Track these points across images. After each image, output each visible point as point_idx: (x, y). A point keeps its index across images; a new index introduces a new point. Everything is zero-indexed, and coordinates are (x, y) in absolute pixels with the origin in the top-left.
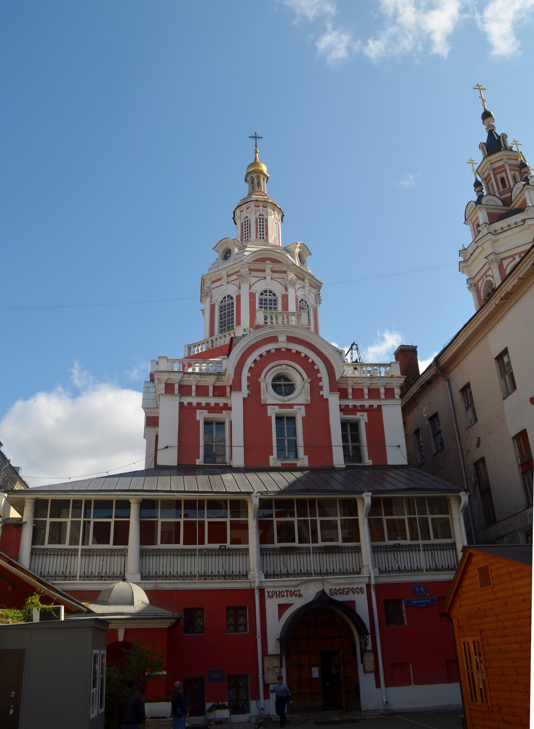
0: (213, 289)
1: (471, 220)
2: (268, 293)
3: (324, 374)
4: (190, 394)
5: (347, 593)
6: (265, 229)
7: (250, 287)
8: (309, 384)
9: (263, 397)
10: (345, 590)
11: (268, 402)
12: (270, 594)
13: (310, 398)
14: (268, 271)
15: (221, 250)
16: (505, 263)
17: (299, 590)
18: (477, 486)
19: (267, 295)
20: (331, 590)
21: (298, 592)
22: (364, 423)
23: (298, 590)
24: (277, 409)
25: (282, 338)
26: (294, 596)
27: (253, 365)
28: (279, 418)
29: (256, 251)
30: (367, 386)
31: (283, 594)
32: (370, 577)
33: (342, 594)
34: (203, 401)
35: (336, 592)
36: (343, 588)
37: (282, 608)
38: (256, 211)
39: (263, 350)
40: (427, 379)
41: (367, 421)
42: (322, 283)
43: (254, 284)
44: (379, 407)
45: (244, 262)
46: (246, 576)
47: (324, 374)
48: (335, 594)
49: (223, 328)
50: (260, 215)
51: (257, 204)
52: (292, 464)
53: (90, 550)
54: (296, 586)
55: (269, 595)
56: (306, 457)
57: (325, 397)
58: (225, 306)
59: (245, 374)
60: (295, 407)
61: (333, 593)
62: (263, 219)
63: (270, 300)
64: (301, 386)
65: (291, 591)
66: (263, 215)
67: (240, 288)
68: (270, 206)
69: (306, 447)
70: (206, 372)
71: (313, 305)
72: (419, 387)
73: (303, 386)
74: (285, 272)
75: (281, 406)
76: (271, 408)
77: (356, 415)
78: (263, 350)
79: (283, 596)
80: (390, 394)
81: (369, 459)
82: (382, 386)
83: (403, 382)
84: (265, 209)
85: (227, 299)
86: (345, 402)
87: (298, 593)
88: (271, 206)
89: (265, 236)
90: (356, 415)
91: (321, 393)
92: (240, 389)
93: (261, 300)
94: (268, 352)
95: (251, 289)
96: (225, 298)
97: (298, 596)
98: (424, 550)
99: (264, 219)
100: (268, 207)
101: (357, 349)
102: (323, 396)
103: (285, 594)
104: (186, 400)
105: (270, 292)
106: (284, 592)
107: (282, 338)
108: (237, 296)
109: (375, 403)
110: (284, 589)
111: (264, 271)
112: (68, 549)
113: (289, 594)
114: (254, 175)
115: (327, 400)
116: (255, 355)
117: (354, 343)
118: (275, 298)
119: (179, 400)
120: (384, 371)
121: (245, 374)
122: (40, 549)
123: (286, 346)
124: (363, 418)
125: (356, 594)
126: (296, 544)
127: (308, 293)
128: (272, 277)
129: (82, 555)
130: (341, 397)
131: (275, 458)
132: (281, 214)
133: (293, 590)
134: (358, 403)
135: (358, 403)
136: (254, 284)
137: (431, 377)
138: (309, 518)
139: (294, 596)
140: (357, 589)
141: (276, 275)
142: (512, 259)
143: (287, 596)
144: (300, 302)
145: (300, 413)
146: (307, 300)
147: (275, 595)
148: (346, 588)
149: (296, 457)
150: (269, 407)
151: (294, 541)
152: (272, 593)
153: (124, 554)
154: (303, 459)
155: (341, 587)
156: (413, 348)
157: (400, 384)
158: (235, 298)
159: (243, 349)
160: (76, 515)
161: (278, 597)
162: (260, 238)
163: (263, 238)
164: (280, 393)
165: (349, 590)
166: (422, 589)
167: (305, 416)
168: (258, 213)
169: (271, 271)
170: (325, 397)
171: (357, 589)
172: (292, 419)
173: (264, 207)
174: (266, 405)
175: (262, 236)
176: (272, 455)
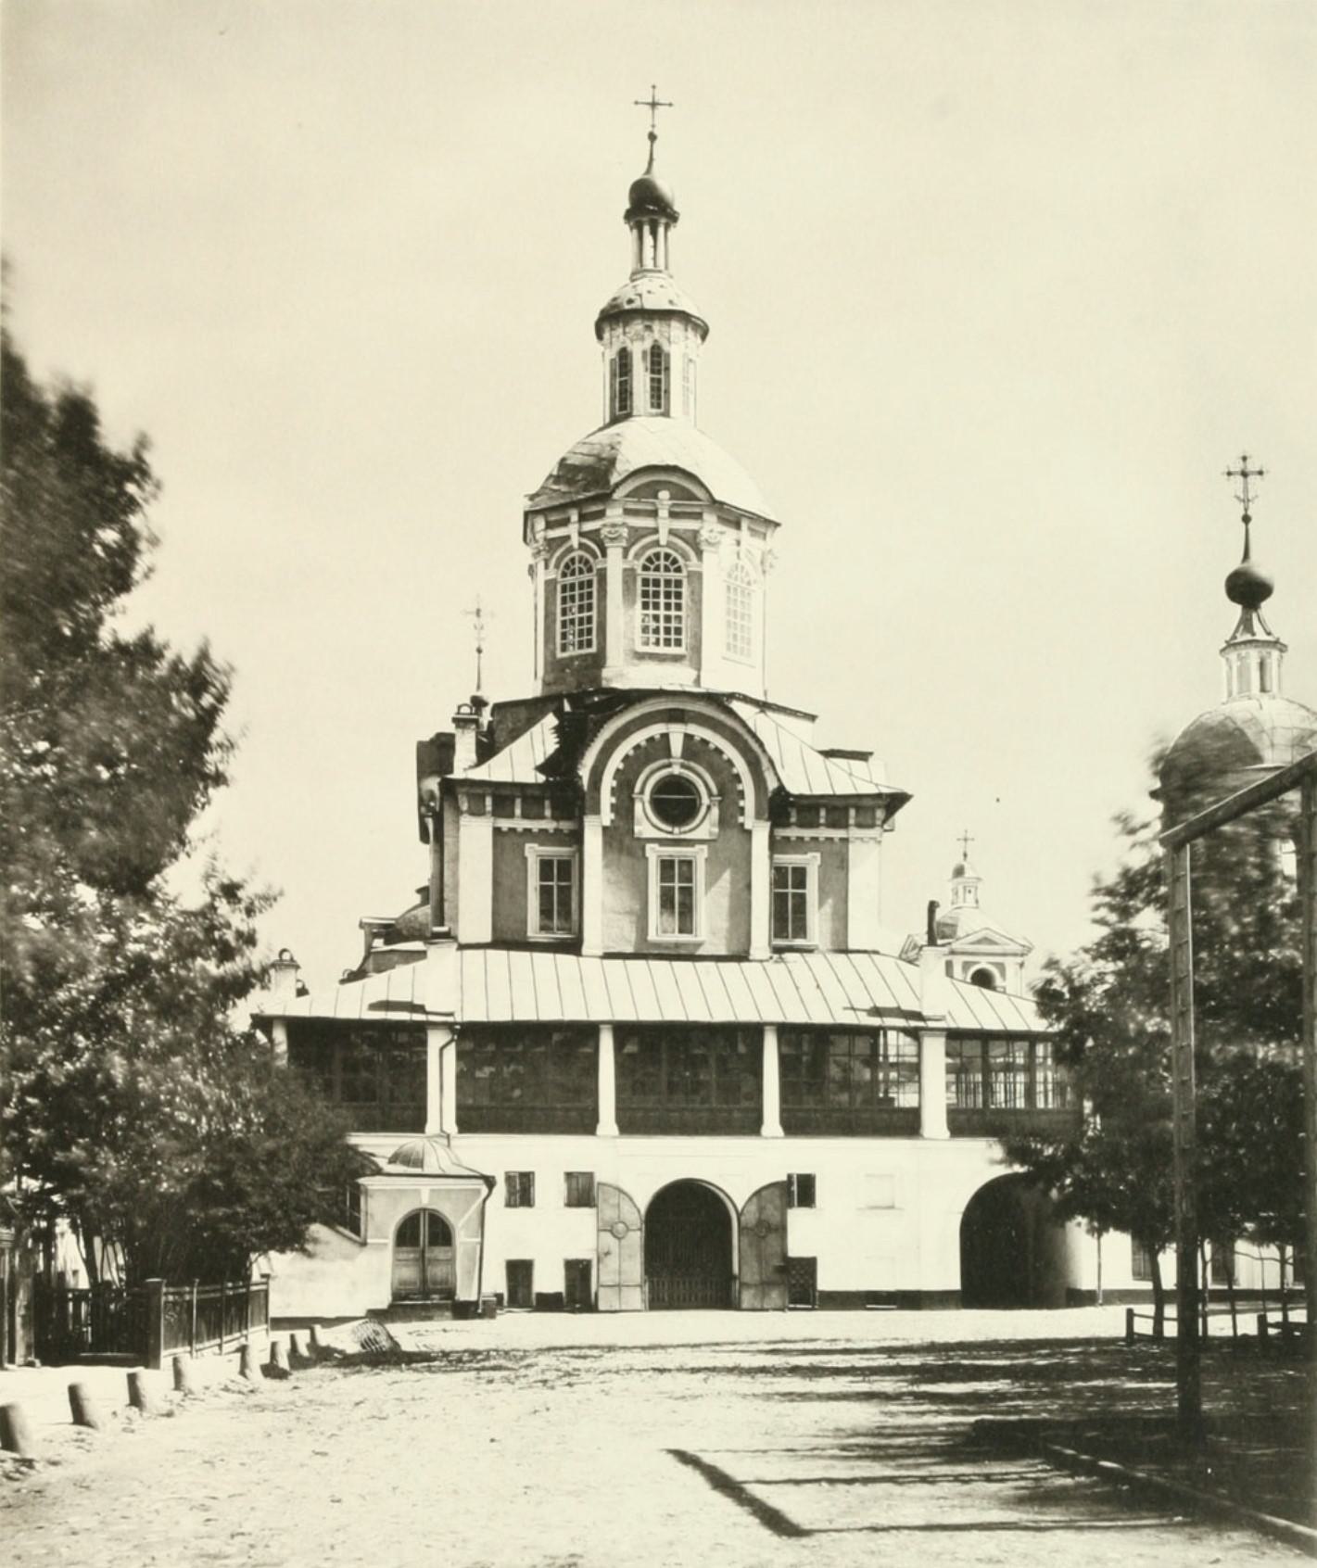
2: (662, 562)
3: (747, 785)
9: (637, 829)
34: (535, 825)
47: (747, 785)
59: (608, 782)
63: (668, 583)
92: (597, 811)
102: (742, 825)
104: (505, 824)
115: (749, 833)
121: (608, 782)
134: (807, 834)
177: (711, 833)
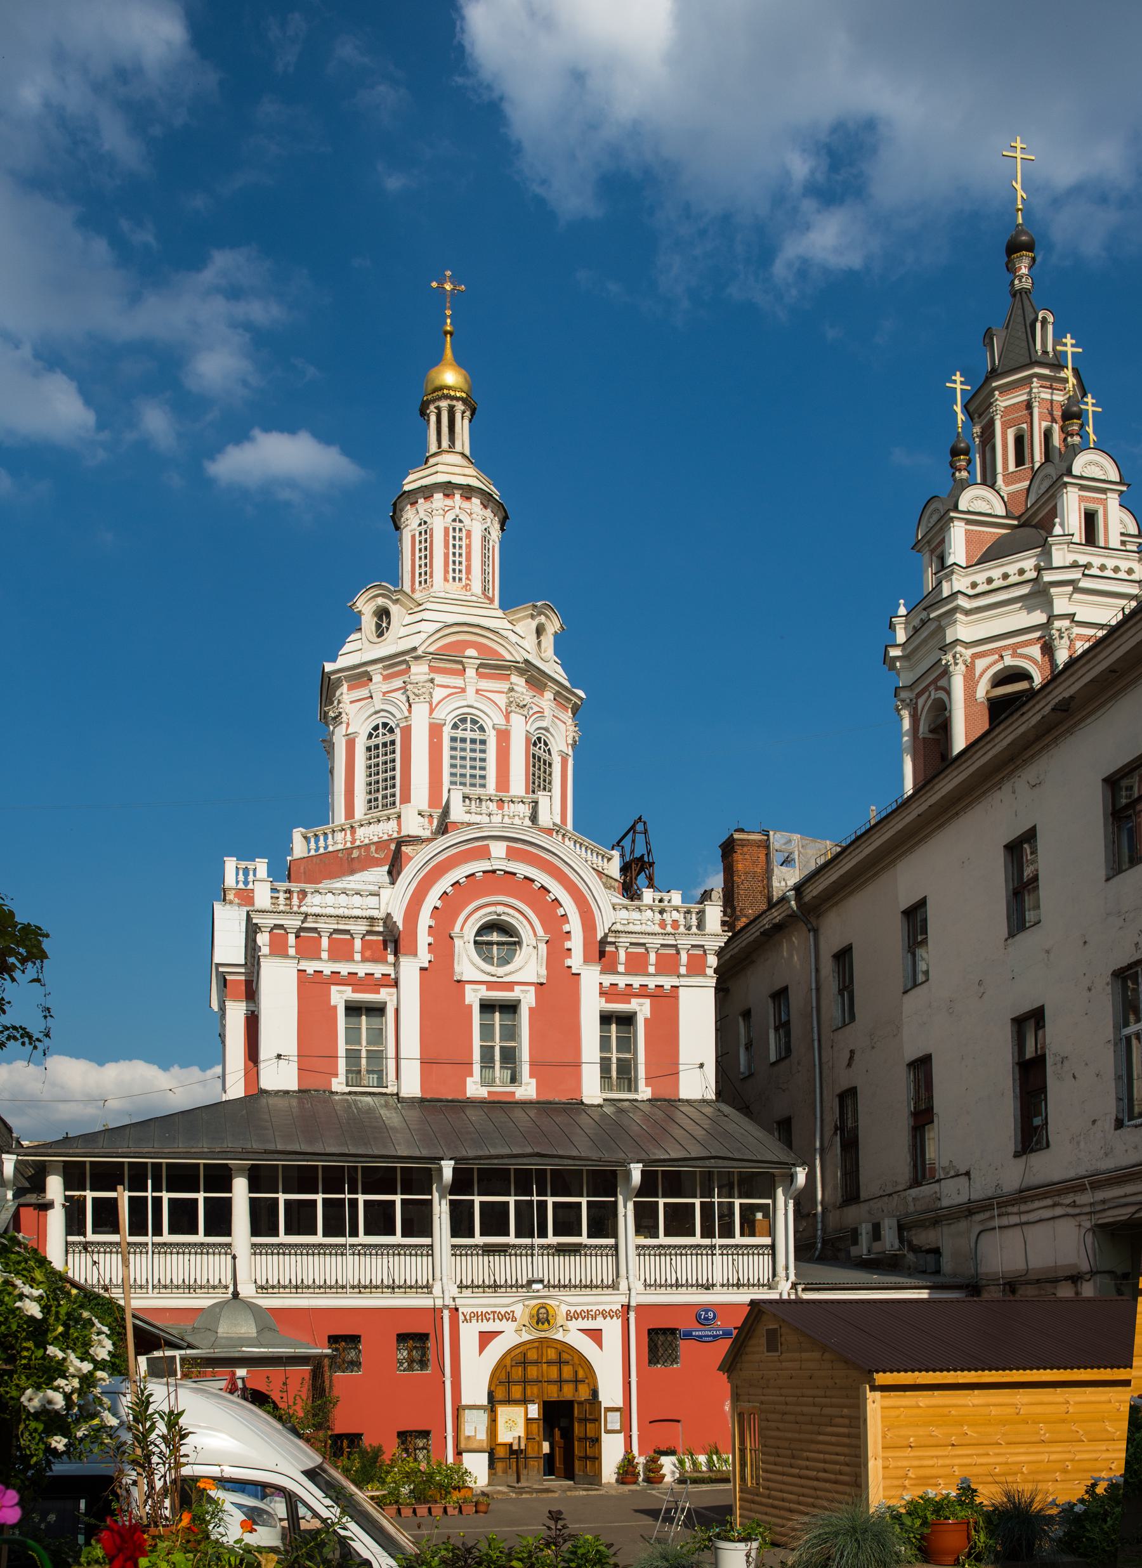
0: (351, 702)
1: (928, 542)
2: (469, 725)
3: (575, 925)
6: (464, 555)
7: (432, 711)
9: (457, 968)
12: (468, 1317)
13: (544, 972)
14: (471, 672)
16: (981, 664)
17: (513, 1312)
27: (439, 904)
28: (487, 1007)
31: (488, 1316)
34: (344, 969)
37: (486, 1338)
41: (649, 1016)
43: (439, 702)
46: (428, 1287)
47: (575, 925)
49: (373, 797)
54: (508, 1306)
56: (534, 1081)
59: (425, 920)
60: (517, 988)
62: (460, 530)
63: (473, 741)
66: (461, 521)
67: (410, 711)
69: (532, 1064)
75: (490, 985)
77: (630, 1003)
78: (459, 873)
79: (488, 1320)
80: (696, 967)
83: (723, 945)
85: (381, 731)
89: (464, 576)
90: (630, 1003)
91: (568, 962)
92: (414, 953)
93: (453, 739)
95: (433, 716)
96: (376, 728)
99: (464, 532)
103: (492, 1316)
104: (310, 967)
105: (474, 722)
109: (667, 982)
110: (489, 1310)
116: (444, 884)
118: (482, 738)
121: (425, 920)
126: (511, 1239)
133: (503, 1311)
134: (637, 981)
135: (637, 981)
136: (439, 702)
138: (535, 1198)
141: (485, 684)
142: (996, 657)
145: (528, 999)
149: (513, 1080)
150: (468, 987)
162: (454, 578)
163: (460, 579)
164: (488, 959)
166: (711, 1315)
170: (574, 971)
175: (457, 575)
176: (472, 1075)
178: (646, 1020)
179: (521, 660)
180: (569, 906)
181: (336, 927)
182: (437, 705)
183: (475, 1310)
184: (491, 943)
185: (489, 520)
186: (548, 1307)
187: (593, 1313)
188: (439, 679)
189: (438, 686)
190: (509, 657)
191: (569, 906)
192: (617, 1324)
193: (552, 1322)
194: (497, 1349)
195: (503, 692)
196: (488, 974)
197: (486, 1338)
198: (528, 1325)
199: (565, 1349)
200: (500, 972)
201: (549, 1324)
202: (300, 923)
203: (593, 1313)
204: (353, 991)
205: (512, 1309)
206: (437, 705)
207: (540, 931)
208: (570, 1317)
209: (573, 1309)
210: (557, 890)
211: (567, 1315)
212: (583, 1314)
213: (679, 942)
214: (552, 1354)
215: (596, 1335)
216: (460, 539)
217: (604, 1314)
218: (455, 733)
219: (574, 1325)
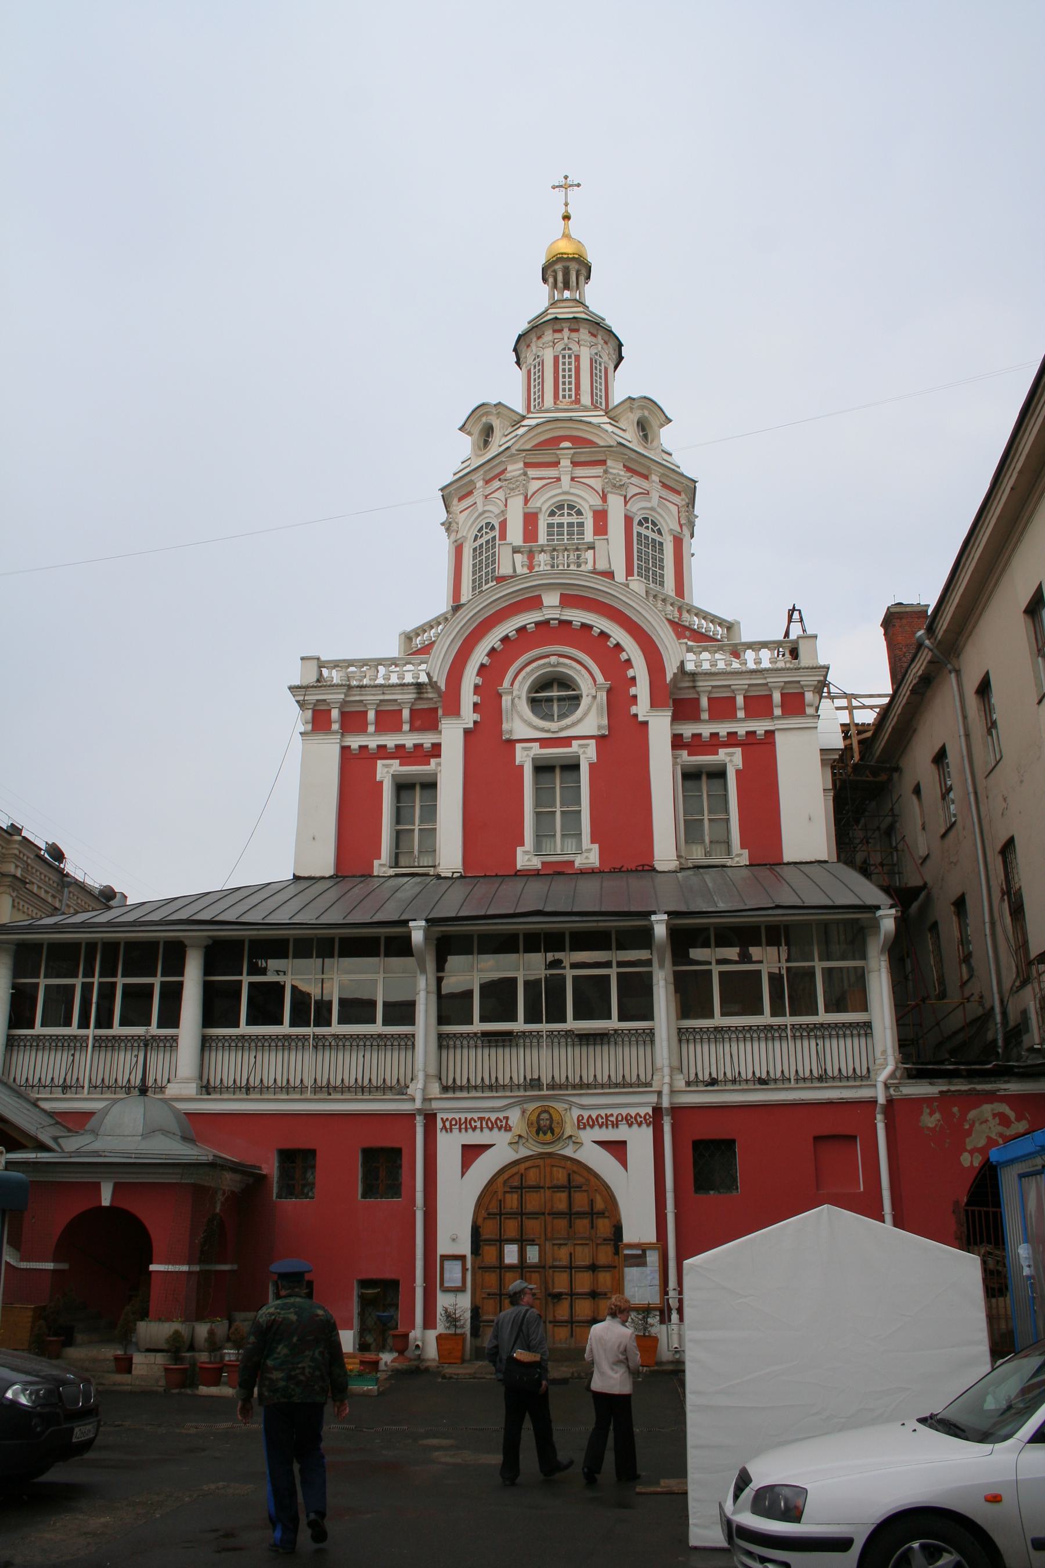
0: (461, 512)
2: (566, 511)
3: (640, 670)
4: (362, 729)
5: (616, 1125)
6: (573, 376)
7: (526, 501)
8: (604, 694)
9: (505, 726)
10: (610, 1118)
11: (515, 737)
12: (448, 1124)
13: (605, 722)
14: (565, 463)
15: (477, 430)
17: (507, 1118)
18: (1004, 900)
19: (564, 516)
20: (581, 1118)
21: (504, 1121)
22: (734, 771)
23: (504, 1118)
24: (536, 749)
25: (551, 599)
26: (496, 1130)
28: (542, 769)
29: (538, 425)
30: (743, 690)
31: (473, 1124)
32: (660, 1093)
33: (604, 1127)
34: (390, 741)
35: (591, 1123)
36: (606, 1115)
37: (471, 1153)
38: (556, 341)
39: (508, 627)
40: (920, 672)
41: (741, 766)
42: (696, 480)
44: (770, 734)
45: (513, 450)
47: (640, 670)
48: (588, 1127)
50: (564, 349)
51: (557, 327)
52: (564, 862)
53: (114, 1037)
55: (444, 1126)
56: (596, 847)
57: (641, 718)
58: (481, 546)
59: (470, 678)
60: (575, 743)
61: (584, 1124)
62: (570, 357)
64: (590, 697)
65: (489, 1119)
66: (570, 349)
67: (506, 506)
68: (585, 328)
70: (413, 681)
71: (671, 530)
72: (908, 693)
73: (595, 697)
74: (603, 462)
76: (523, 748)
77: (717, 754)
78: (508, 627)
79: (474, 1129)
81: (742, 847)
82: (775, 688)
84: (574, 335)
86: (688, 730)
87: (504, 1123)
88: (587, 326)
90: (717, 754)
91: (634, 710)
93: (550, 526)
94: (522, 630)
95: (528, 505)
97: (503, 1129)
98: (794, 1037)
100: (582, 330)
101: (801, 620)
102: (636, 716)
103: (478, 1124)
104: (355, 742)
105: (571, 507)
106: (475, 1122)
107: (551, 599)
108: (500, 523)
109: (760, 727)
110: (476, 1116)
111: (556, 464)
112: (75, 1036)
113: (484, 1125)
114: (558, 267)
115: (645, 724)
116: (492, 639)
117: (794, 607)
119: (341, 741)
120: (770, 656)
121: (470, 678)
122: (26, 1036)
123: (557, 616)
124: (732, 759)
125: (635, 1126)
126: (519, 1025)
127: (659, 504)
128: (574, 475)
129: (94, 1047)
130: (676, 718)
131: (528, 851)
132: (613, 344)
133: (493, 1117)
134: (723, 729)
135: (723, 729)
137: (926, 667)
139: (496, 1130)
140: (638, 1117)
141: (580, 472)
143: (482, 1129)
144: (640, 524)
145: (587, 754)
146: (656, 519)
147: (458, 1126)
148: (612, 1115)
150: (518, 746)
151: (514, 1019)
152: (451, 1123)
153: (172, 1042)
154: (589, 850)
155: (603, 1113)
156: (919, 609)
157: (816, 682)
158: (497, 527)
159: (465, 627)
160: (109, 970)
161: (463, 1130)
162: (564, 397)
163: (570, 396)
165: (620, 1118)
167: (596, 761)
168: (560, 346)
169: (571, 463)
170: (641, 718)
171: (638, 1117)
172: (572, 767)
173: (572, 330)
174: (511, 743)
176: (523, 845)
177: (600, 727)
178: (738, 772)
179: (615, 444)
180: (632, 650)
181: (381, 697)
182: (532, 496)
183: (457, 1116)
184: (549, 700)
185: (600, 347)
186: (552, 1111)
187: (613, 1119)
188: (532, 472)
189: (533, 479)
190: (602, 443)
191: (632, 650)
192: (648, 1132)
193: (557, 1130)
194: (486, 1167)
195: (600, 477)
196: (543, 730)
197: (471, 1153)
198: (524, 1134)
199: (575, 1168)
200: (553, 727)
201: (553, 1133)
202: (342, 696)
203: (613, 1119)
204: (401, 765)
205: (505, 1114)
206: (532, 496)
207: (600, 678)
208: (583, 1124)
209: (586, 1114)
210: (618, 635)
211: (579, 1121)
212: (600, 1120)
213: (769, 680)
214: (560, 1176)
215: (617, 1149)
216: (570, 364)
217: (630, 1121)
218: (550, 520)
219: (588, 1136)
